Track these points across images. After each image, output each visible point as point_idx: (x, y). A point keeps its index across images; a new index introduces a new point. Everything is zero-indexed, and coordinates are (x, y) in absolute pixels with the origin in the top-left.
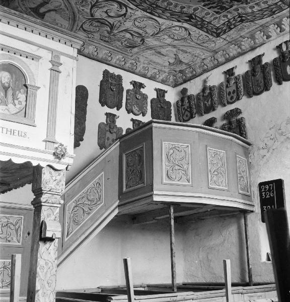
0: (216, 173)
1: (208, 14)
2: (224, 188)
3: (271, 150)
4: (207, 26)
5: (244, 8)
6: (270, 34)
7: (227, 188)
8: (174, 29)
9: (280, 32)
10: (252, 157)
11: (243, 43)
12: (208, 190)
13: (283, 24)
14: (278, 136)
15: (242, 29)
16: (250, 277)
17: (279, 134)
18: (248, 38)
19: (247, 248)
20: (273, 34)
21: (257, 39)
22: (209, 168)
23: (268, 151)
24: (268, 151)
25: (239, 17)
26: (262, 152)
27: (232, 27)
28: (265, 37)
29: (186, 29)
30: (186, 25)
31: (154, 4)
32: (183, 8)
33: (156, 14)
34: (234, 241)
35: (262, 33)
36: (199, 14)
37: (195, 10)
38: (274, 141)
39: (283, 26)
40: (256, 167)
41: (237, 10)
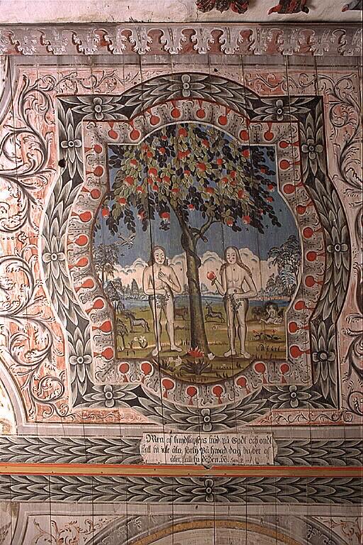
1: (285, 164)
4: (310, 138)
5: (233, 129)
6: (241, 39)
8: (354, 179)
9: (222, 33)
11: (297, 48)
13: (210, 44)
15: (276, 83)
18: (282, 54)
20: (236, 33)
21: (267, 41)
25: (252, 114)
27: (279, 102)
28: (252, 38)
29: (341, 161)
30: (333, 170)
31: (326, 251)
32: (301, 209)
33: (344, 231)
35: (253, 47)
36: (295, 176)
37: (290, 189)
39: (212, 41)
41: (244, 135)
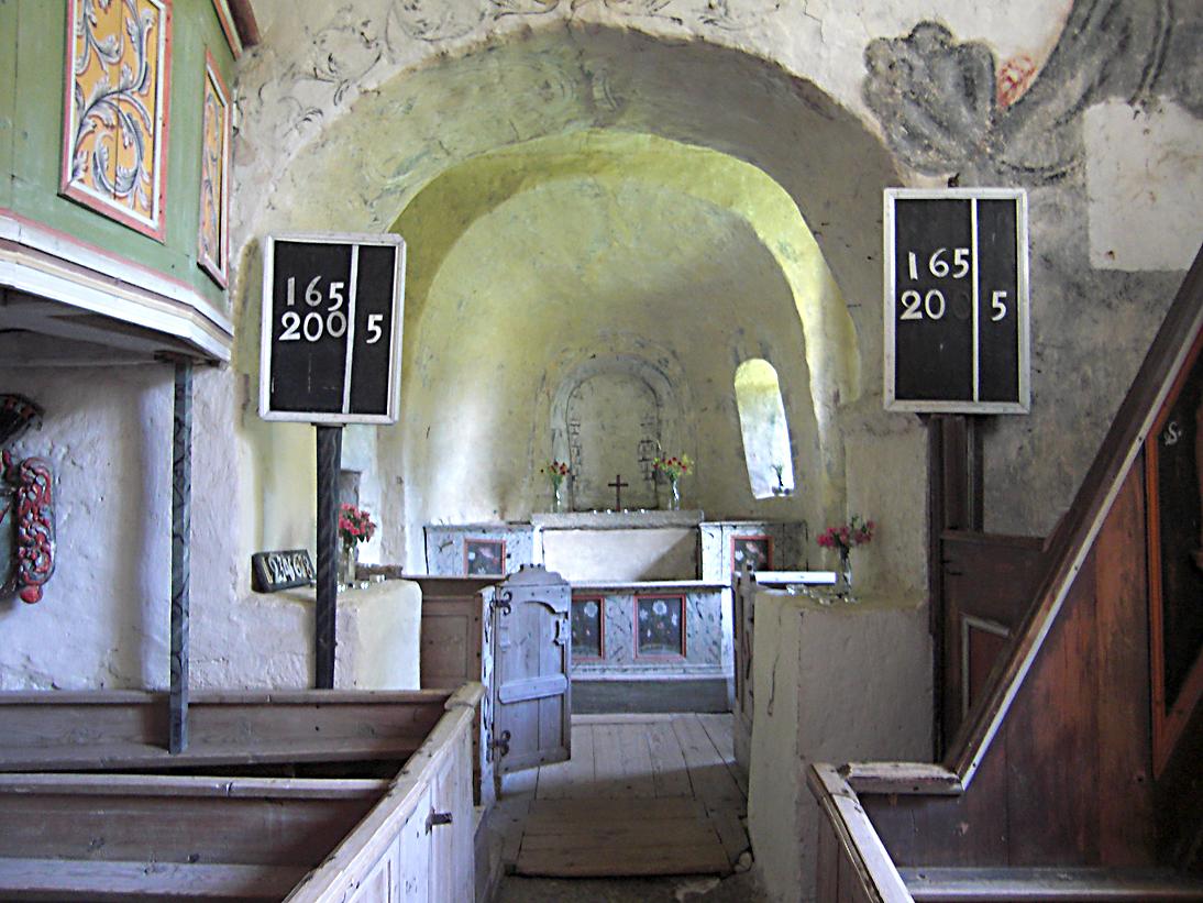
0: (105, 112)
2: (144, 219)
3: (354, 90)
7: (154, 224)
10: (251, 105)
12: (53, 206)
14: (395, 32)
16: (177, 674)
17: (404, 25)
19: (178, 538)
22: (75, 66)
23: (339, 96)
24: (339, 96)
26: (304, 90)
34: (95, 496)
38: (373, 53)
40: (263, 156)
